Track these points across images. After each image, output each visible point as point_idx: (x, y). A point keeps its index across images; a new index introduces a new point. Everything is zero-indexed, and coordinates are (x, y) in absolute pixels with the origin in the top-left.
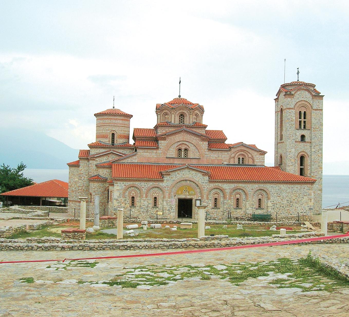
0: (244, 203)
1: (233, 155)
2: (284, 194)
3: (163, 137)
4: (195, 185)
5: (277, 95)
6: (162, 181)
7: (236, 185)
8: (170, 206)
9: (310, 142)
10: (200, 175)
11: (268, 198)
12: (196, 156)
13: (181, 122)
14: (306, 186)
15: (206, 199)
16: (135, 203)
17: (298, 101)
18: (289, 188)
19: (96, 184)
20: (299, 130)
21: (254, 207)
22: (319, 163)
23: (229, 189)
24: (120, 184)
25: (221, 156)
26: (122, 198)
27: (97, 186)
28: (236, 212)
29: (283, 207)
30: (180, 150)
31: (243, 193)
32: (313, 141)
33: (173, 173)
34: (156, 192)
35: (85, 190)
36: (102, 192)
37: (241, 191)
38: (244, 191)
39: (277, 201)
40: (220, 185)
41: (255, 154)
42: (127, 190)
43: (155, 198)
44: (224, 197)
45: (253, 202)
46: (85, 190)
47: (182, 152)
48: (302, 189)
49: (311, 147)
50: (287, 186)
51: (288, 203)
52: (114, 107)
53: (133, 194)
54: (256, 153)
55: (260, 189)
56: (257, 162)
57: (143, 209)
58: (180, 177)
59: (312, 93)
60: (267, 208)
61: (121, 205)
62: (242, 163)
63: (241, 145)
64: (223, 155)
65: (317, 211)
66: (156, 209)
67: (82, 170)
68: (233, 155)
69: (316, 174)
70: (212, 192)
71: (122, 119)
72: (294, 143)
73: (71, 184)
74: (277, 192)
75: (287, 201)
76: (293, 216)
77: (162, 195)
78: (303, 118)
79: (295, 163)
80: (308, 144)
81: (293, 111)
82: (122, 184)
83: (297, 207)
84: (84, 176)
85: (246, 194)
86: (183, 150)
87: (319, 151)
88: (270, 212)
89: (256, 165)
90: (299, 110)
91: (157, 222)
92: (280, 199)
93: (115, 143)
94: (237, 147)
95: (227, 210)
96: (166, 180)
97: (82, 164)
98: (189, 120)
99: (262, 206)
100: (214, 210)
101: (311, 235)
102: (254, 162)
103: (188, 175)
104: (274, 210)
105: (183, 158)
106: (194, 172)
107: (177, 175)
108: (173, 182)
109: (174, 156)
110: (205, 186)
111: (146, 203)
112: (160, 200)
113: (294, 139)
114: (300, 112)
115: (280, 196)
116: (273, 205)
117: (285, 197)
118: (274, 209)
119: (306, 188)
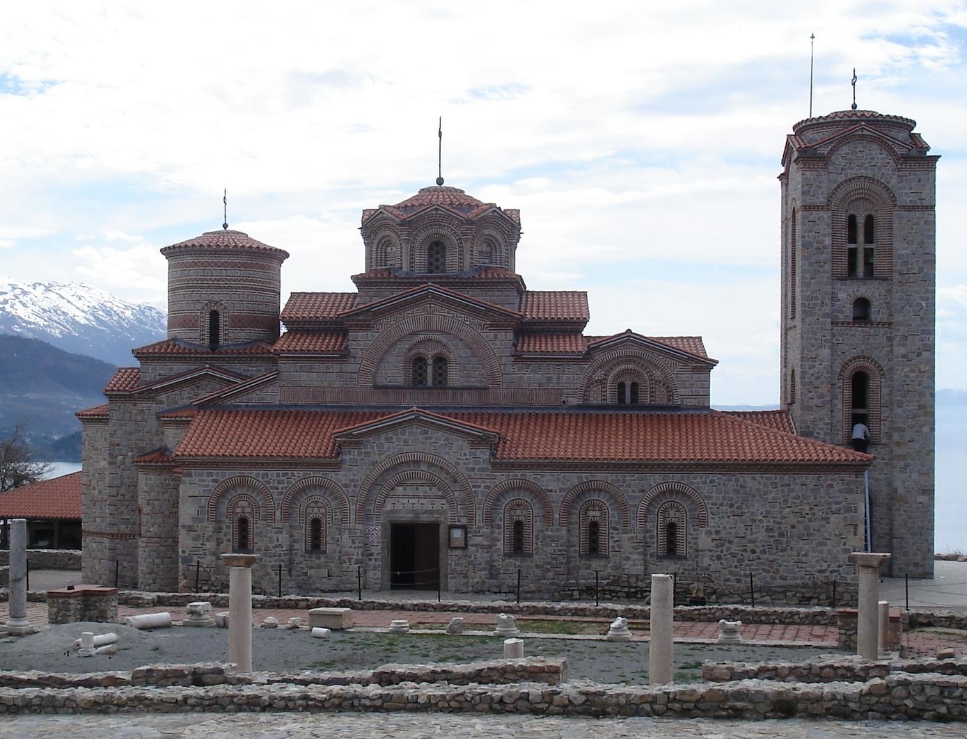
0: (616, 539)
1: (599, 375)
2: (757, 507)
3: (359, 320)
4: (446, 479)
5: (783, 164)
6: (337, 466)
7: (585, 476)
8: (360, 551)
9: (890, 324)
10: (461, 442)
11: (703, 523)
12: (472, 380)
13: (437, 268)
14: (838, 481)
15: (482, 525)
16: (250, 537)
17: (841, 178)
18: (775, 485)
19: (154, 478)
20: (848, 282)
21: (653, 549)
22: (922, 395)
23: (561, 490)
24: (198, 478)
25: (558, 379)
26: (206, 524)
27: (157, 482)
28: (586, 569)
29: (753, 552)
30: (419, 361)
31: (610, 505)
32: (898, 318)
33: (371, 439)
34: (316, 502)
35: (126, 499)
36: (173, 505)
37: (602, 498)
38: (612, 496)
39: (733, 531)
40: (530, 476)
41: (675, 370)
42: (222, 495)
43: (316, 523)
44: (547, 519)
45: (648, 535)
46: (126, 499)
47: (429, 367)
48: (822, 490)
49: (890, 339)
50: (767, 479)
51: (773, 537)
52: (225, 226)
53: (243, 508)
55: (671, 492)
56: (683, 395)
57: (276, 558)
59: (895, 149)
60: (697, 556)
61: (204, 547)
63: (626, 341)
65: (916, 565)
66: (319, 558)
67: (116, 431)
68: (598, 373)
69: (909, 434)
70: (503, 500)
72: (829, 326)
73: (91, 478)
74: (731, 499)
75: (769, 530)
76: (789, 582)
77: (338, 510)
78: (861, 237)
79: (834, 397)
80: (882, 331)
81: (825, 216)
82: (205, 478)
83: (803, 553)
84: (124, 452)
85: (622, 508)
86: (430, 361)
87: (921, 353)
88: (707, 569)
89: (678, 408)
90: (846, 211)
91: (276, 603)
92: (742, 525)
93: (221, 342)
94: (614, 345)
95: (555, 562)
96: (348, 464)
97: (115, 412)
98: (464, 258)
99: (681, 548)
100: (512, 560)
101: (508, 670)
102: (671, 394)
103: (422, 443)
104: (721, 564)
106: (440, 434)
107: (386, 445)
108: (372, 468)
109: (400, 381)
110: (479, 480)
111: (284, 538)
112: (330, 527)
113: (827, 315)
114: (852, 220)
115: (743, 514)
116: (717, 546)
117: (760, 517)
118: (719, 558)
119: (838, 485)
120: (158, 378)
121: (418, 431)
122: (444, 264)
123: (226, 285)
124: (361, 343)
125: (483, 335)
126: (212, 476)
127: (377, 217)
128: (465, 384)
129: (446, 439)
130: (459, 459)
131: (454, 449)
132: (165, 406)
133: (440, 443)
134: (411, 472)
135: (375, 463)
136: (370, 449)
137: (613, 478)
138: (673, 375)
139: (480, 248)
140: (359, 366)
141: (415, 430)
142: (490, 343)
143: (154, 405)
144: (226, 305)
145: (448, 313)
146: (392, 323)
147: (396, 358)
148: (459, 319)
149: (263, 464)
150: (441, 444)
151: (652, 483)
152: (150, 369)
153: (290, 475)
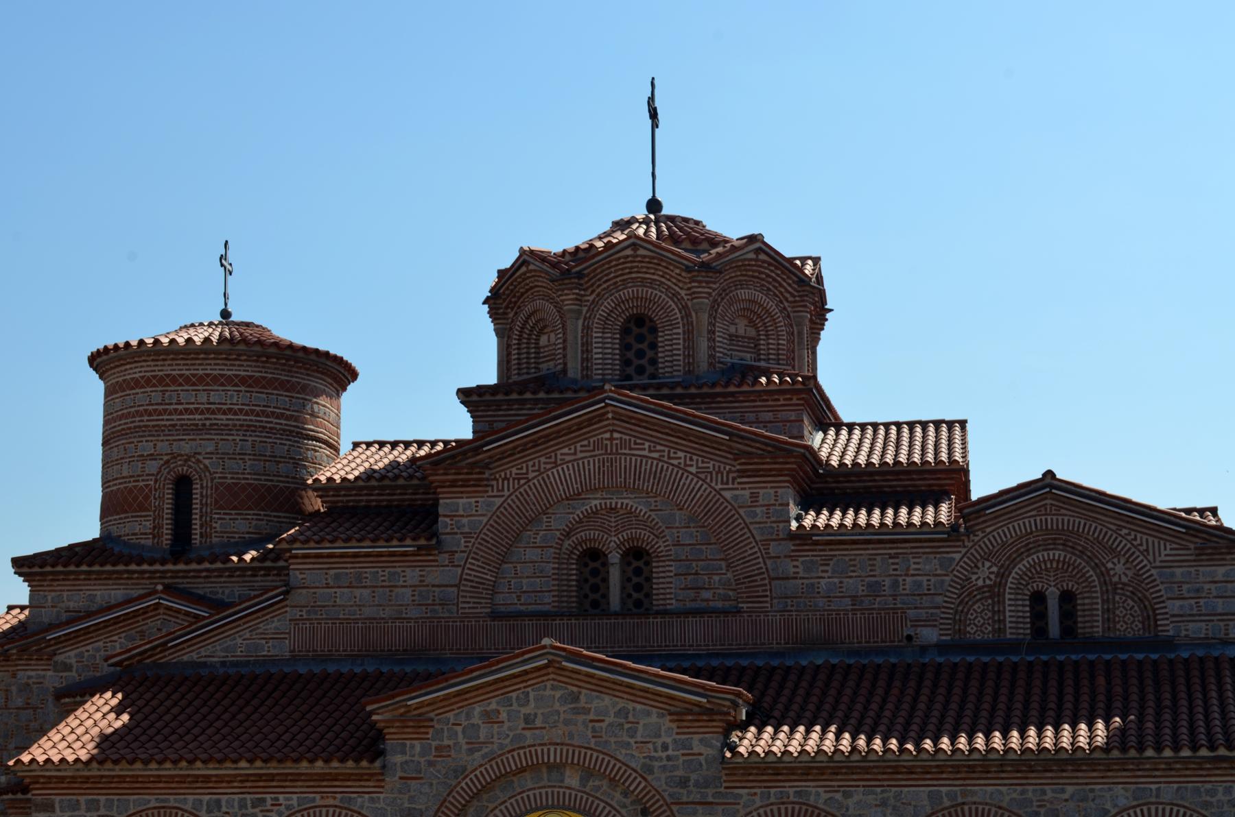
1: (985, 574)
4: (624, 806)
10: (654, 719)
12: (706, 595)
13: (640, 370)
25: (895, 584)
33: (451, 715)
54: (1166, 552)
58: (501, 746)
62: (1068, 630)
63: (1043, 497)
64: (909, 579)
71: (243, 381)
86: (615, 558)
89: (1169, 644)
93: (196, 539)
96: (399, 774)
103: (567, 722)
105: (616, 614)
106: (607, 700)
109: (548, 602)
120: (64, 617)
121: (558, 694)
122: (653, 362)
123: (208, 423)
124: (465, 520)
125: (727, 494)
126: (98, 810)
127: (518, 274)
128: (689, 605)
129: (623, 713)
130: (651, 758)
131: (639, 734)
132: (74, 674)
133: (608, 720)
134: (543, 791)
135: (461, 772)
136: (449, 738)
137: (1014, 795)
138: (1153, 571)
139: (732, 329)
140: (459, 570)
141: (548, 692)
142: (742, 511)
143: (50, 673)
144: (207, 462)
145: (650, 451)
146: (531, 475)
147: (539, 550)
148: (675, 462)
149: (207, 778)
150: (611, 725)
151: (1108, 806)
152: (49, 598)
153: (269, 802)
